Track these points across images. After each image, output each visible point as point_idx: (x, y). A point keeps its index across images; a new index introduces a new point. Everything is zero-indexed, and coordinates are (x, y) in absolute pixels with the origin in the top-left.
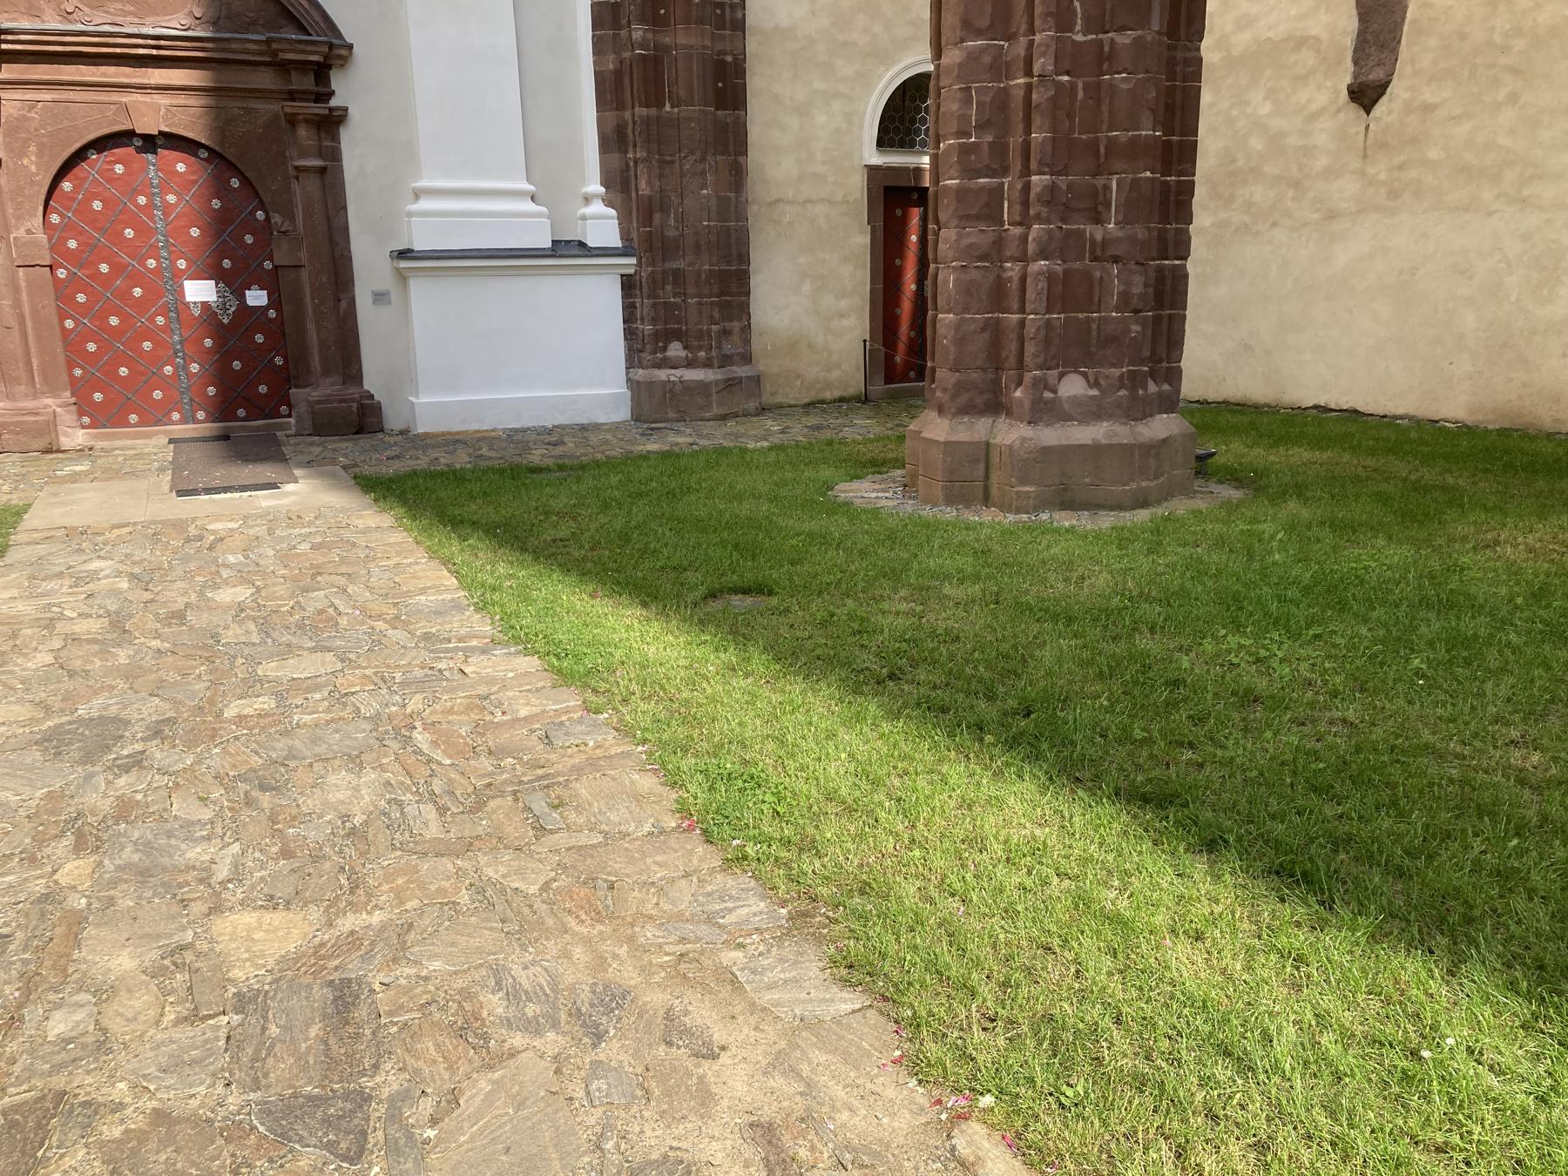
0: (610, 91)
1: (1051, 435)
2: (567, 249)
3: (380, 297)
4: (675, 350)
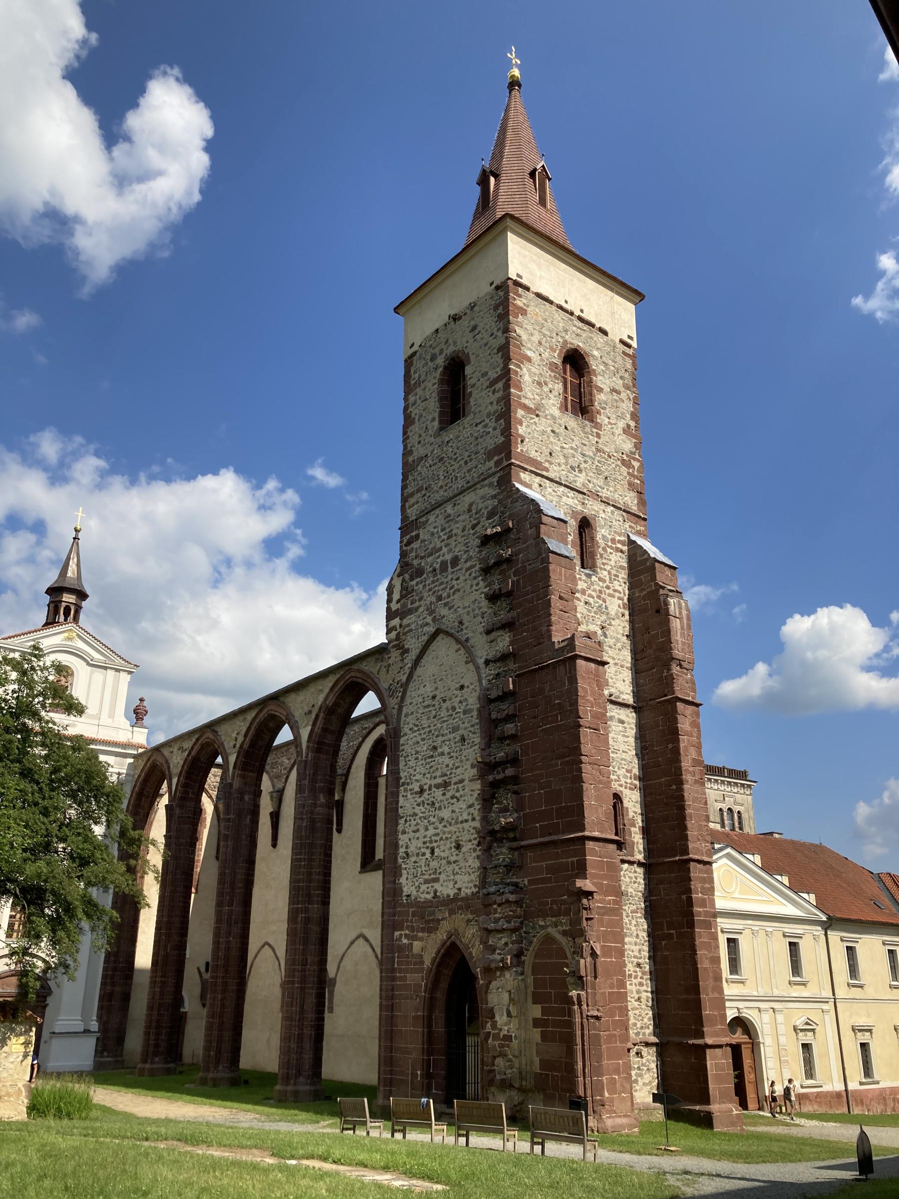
1: (153, 1066)
2: (87, 1031)
3: (45, 1042)
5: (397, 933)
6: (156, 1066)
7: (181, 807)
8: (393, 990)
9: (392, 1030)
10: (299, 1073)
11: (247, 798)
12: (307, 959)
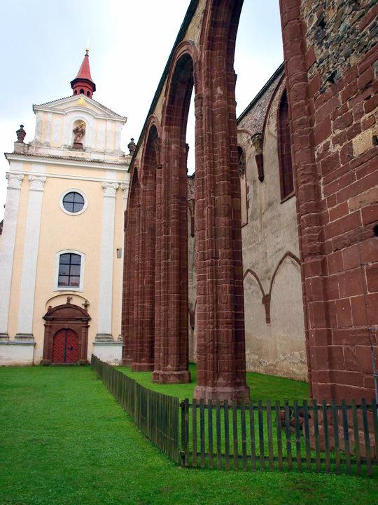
0: (123, 323)
4: (128, 356)
5: (320, 147)
6: (143, 364)
7: (145, 185)
8: (321, 238)
9: (327, 306)
10: (217, 374)
11: (173, 147)
12: (217, 252)
